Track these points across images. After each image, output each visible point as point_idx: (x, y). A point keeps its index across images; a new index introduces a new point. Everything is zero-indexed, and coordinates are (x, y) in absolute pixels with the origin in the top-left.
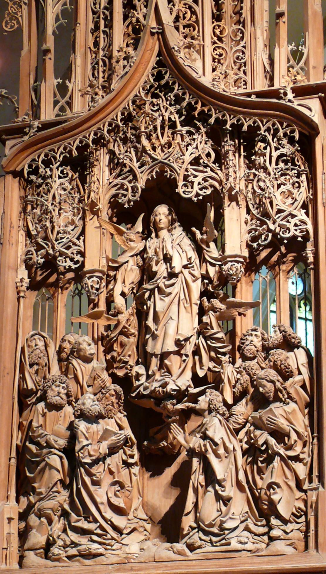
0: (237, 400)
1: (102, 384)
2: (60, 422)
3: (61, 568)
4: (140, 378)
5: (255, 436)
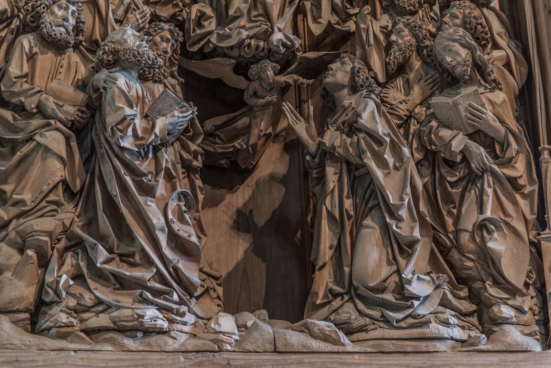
0: (390, 77)
1: (140, 21)
2: (59, 76)
3: (72, 353)
4: (206, 23)
5: (441, 138)
